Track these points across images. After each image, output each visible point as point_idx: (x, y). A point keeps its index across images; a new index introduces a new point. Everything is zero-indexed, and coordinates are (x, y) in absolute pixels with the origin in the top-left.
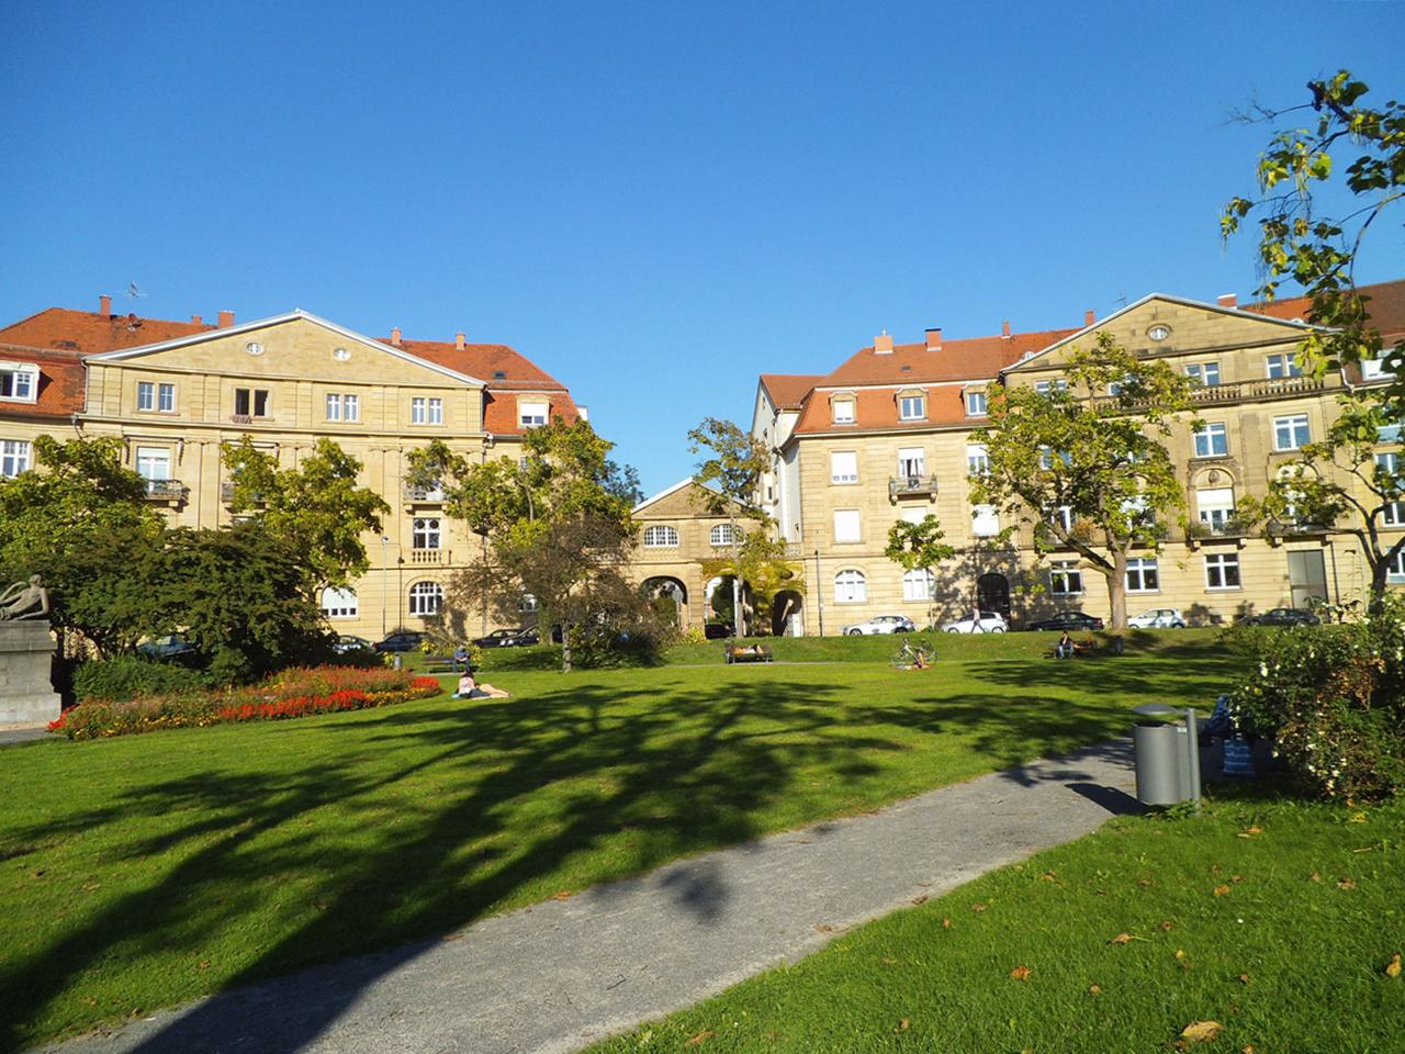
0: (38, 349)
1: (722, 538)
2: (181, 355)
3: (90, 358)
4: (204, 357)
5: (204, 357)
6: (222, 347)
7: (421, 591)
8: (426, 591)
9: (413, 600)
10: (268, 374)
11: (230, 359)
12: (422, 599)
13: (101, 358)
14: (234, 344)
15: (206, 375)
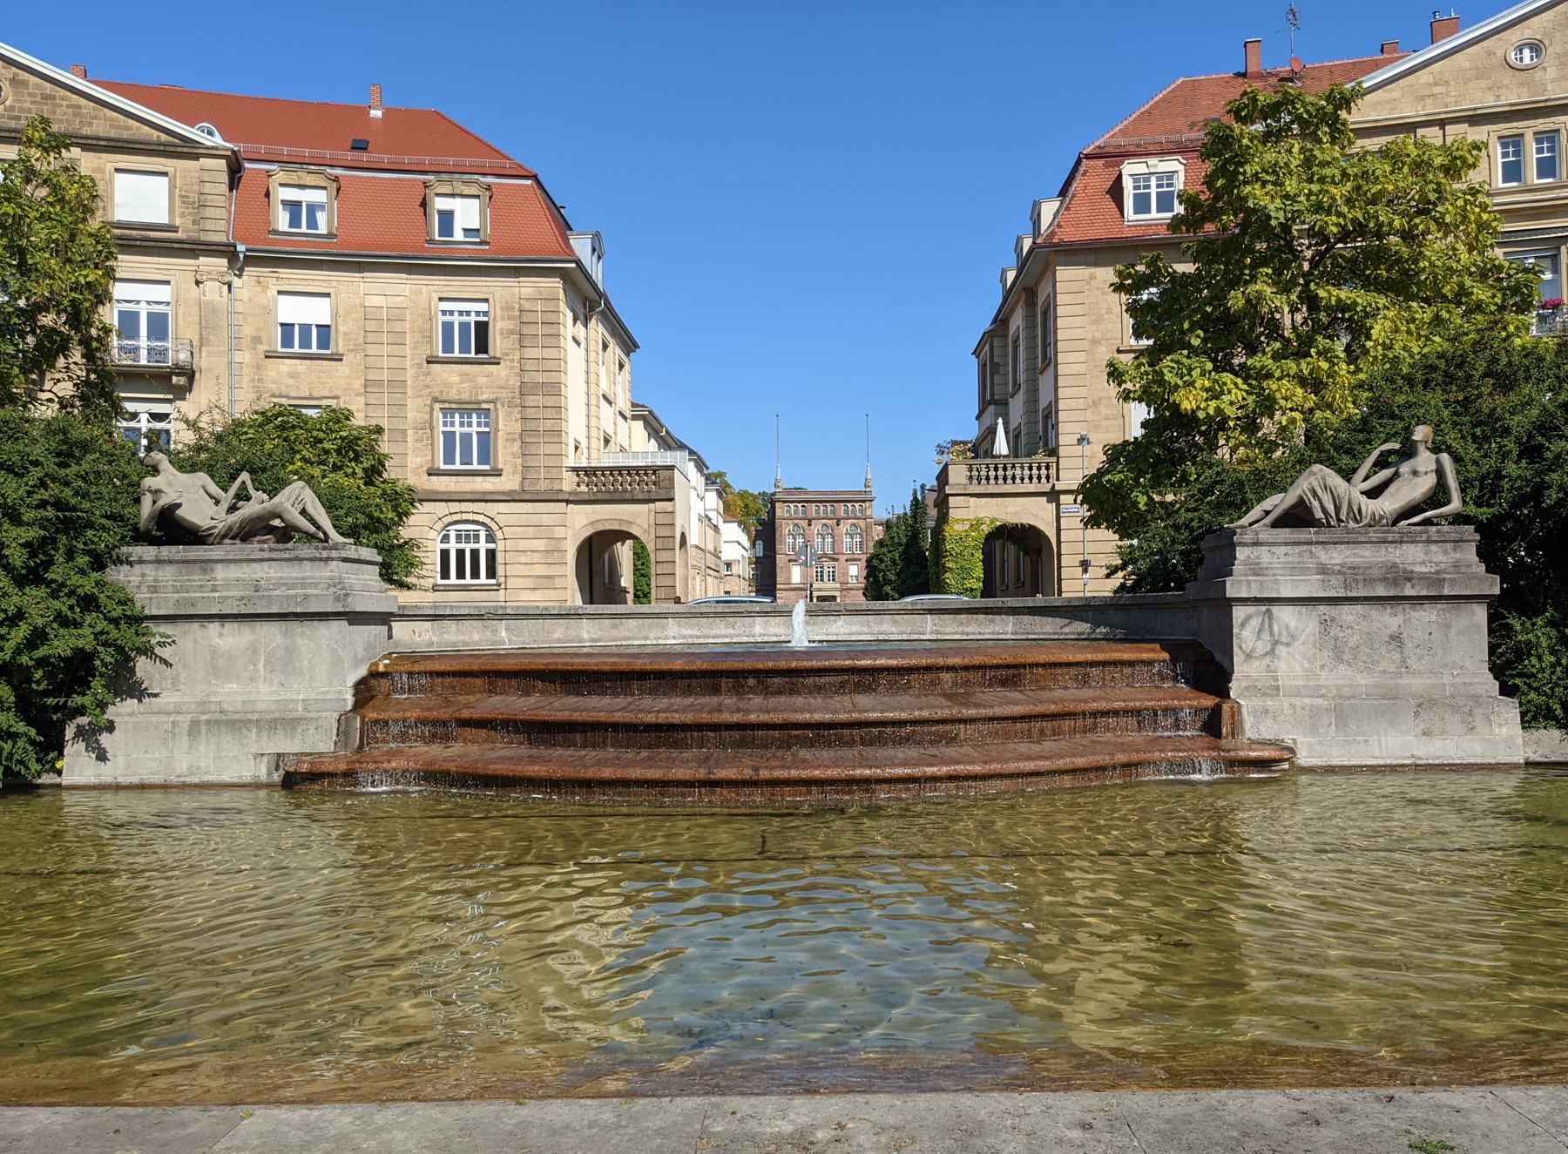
0: (1175, 137)
2: (1395, 95)
4: (1437, 90)
5: (1437, 90)
11: (1483, 83)
14: (1489, 53)
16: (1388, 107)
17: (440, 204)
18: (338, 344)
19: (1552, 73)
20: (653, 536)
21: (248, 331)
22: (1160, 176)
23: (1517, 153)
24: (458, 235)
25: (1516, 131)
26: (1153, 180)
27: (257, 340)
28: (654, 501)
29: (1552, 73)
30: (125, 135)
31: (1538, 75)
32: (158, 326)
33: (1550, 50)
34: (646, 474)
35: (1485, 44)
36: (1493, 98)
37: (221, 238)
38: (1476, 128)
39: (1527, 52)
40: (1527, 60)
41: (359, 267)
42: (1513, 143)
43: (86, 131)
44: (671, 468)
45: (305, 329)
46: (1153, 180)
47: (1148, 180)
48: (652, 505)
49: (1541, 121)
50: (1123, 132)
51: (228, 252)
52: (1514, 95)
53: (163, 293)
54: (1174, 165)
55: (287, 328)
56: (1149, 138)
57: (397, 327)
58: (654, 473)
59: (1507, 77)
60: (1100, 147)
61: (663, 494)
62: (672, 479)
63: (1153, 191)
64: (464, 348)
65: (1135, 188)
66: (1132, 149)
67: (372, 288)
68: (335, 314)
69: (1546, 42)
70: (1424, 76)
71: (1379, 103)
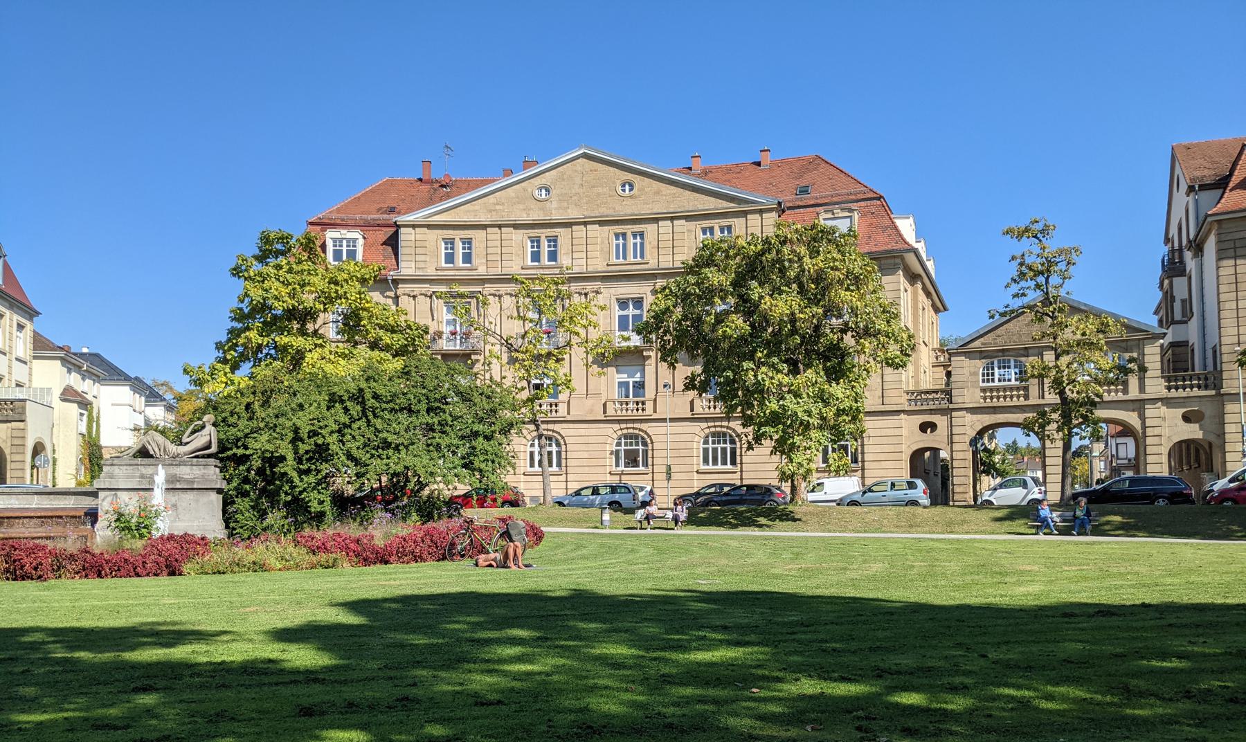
1: (1013, 379)
2: (477, 207)
3: (401, 219)
5: (498, 207)
6: (513, 195)
7: (713, 443)
8: (719, 443)
9: (706, 451)
10: (557, 216)
11: (521, 207)
12: (715, 450)
13: (411, 218)
15: (500, 226)
16: (473, 214)
19: (555, 204)
20: (9, 444)
22: (348, 240)
23: (538, 247)
25: (537, 235)
26: (345, 242)
28: (10, 421)
29: (555, 204)
31: (548, 204)
33: (554, 192)
34: (6, 404)
35: (523, 184)
36: (525, 215)
38: (517, 231)
39: (543, 191)
40: (544, 196)
42: (536, 241)
44: (24, 401)
46: (345, 242)
47: (341, 242)
48: (9, 424)
49: (549, 230)
50: (338, 210)
52: (536, 215)
54: (356, 234)
56: (351, 216)
58: (12, 403)
59: (533, 204)
60: (320, 218)
61: (17, 417)
62: (24, 408)
63: (345, 249)
65: (335, 246)
66: (338, 221)
69: (553, 187)
70: (491, 199)
71: (469, 211)
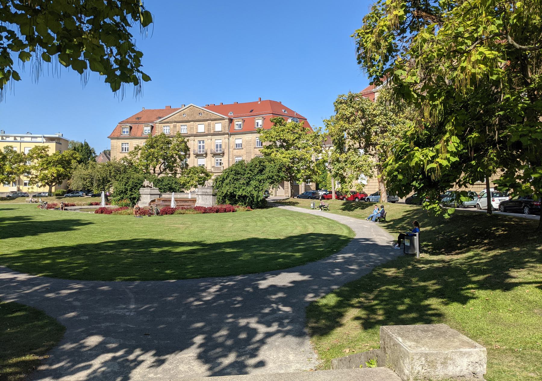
17: (257, 121)
18: (243, 146)
21: (231, 146)
24: (259, 126)
27: (232, 147)
30: (216, 118)
32: (221, 145)
37: (227, 132)
41: (245, 134)
43: (212, 118)
45: (239, 144)
51: (228, 134)
53: (221, 141)
55: (237, 144)
57: (250, 143)
64: (260, 146)
67: (246, 137)
68: (242, 142)
